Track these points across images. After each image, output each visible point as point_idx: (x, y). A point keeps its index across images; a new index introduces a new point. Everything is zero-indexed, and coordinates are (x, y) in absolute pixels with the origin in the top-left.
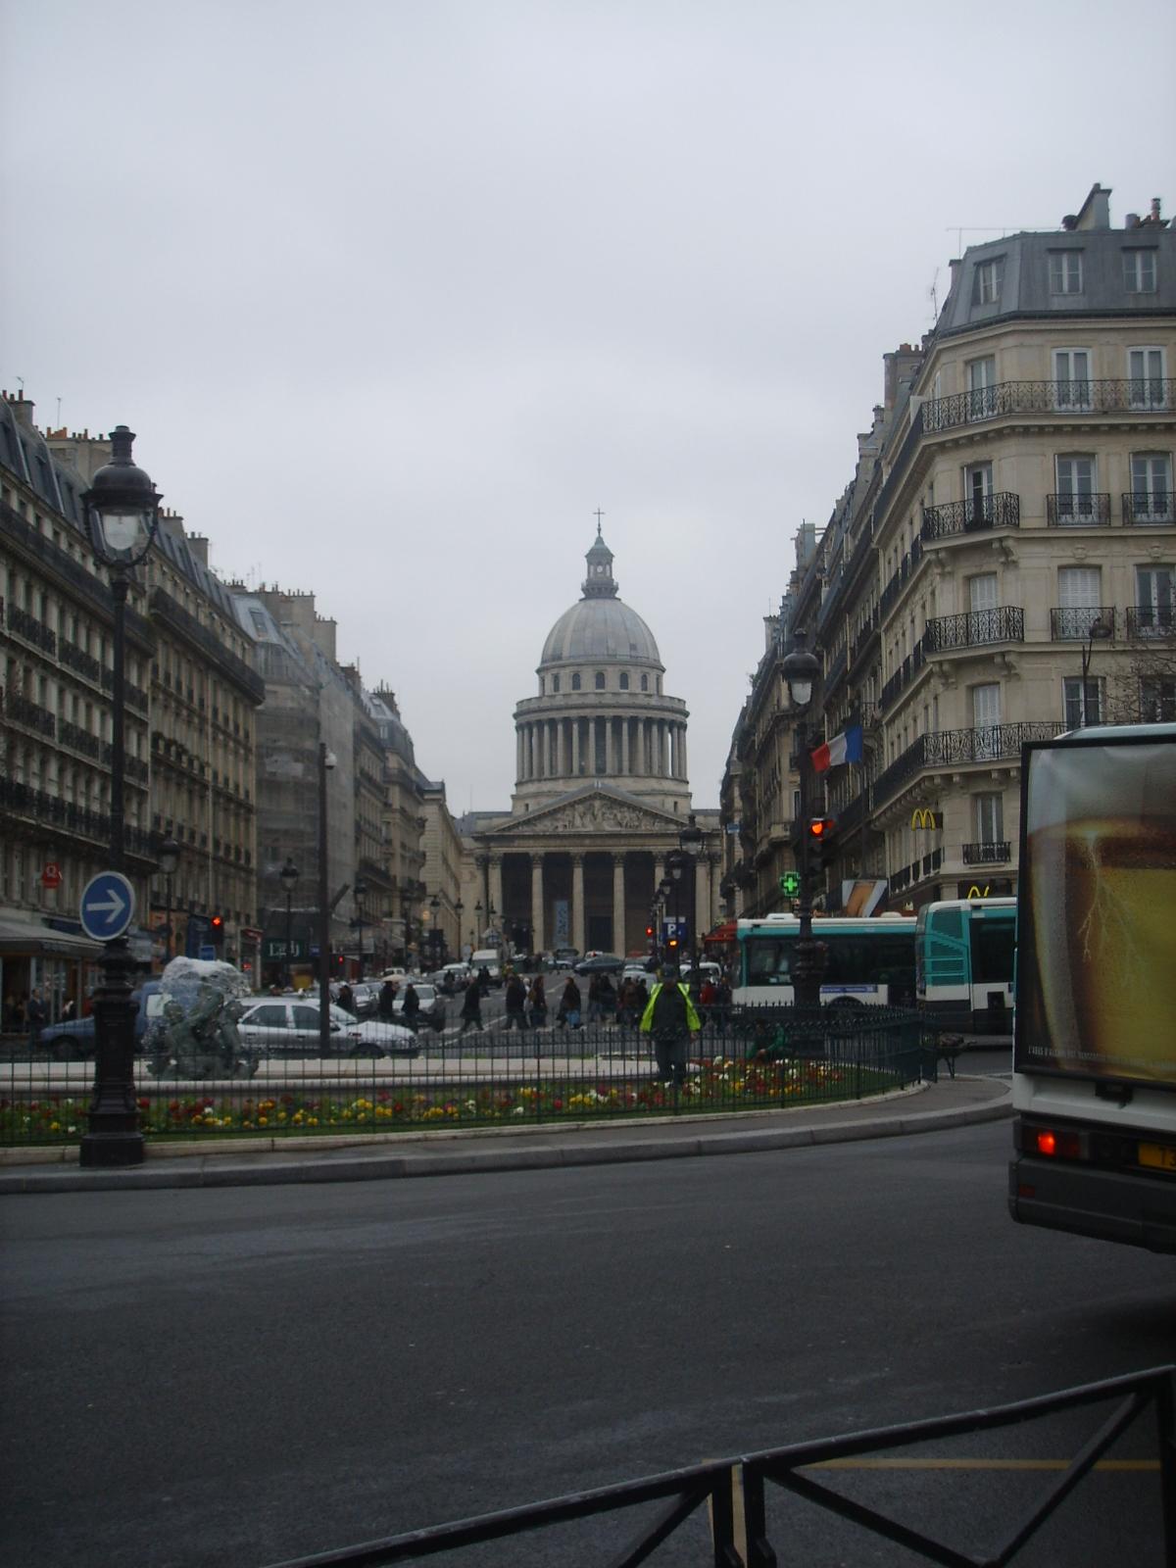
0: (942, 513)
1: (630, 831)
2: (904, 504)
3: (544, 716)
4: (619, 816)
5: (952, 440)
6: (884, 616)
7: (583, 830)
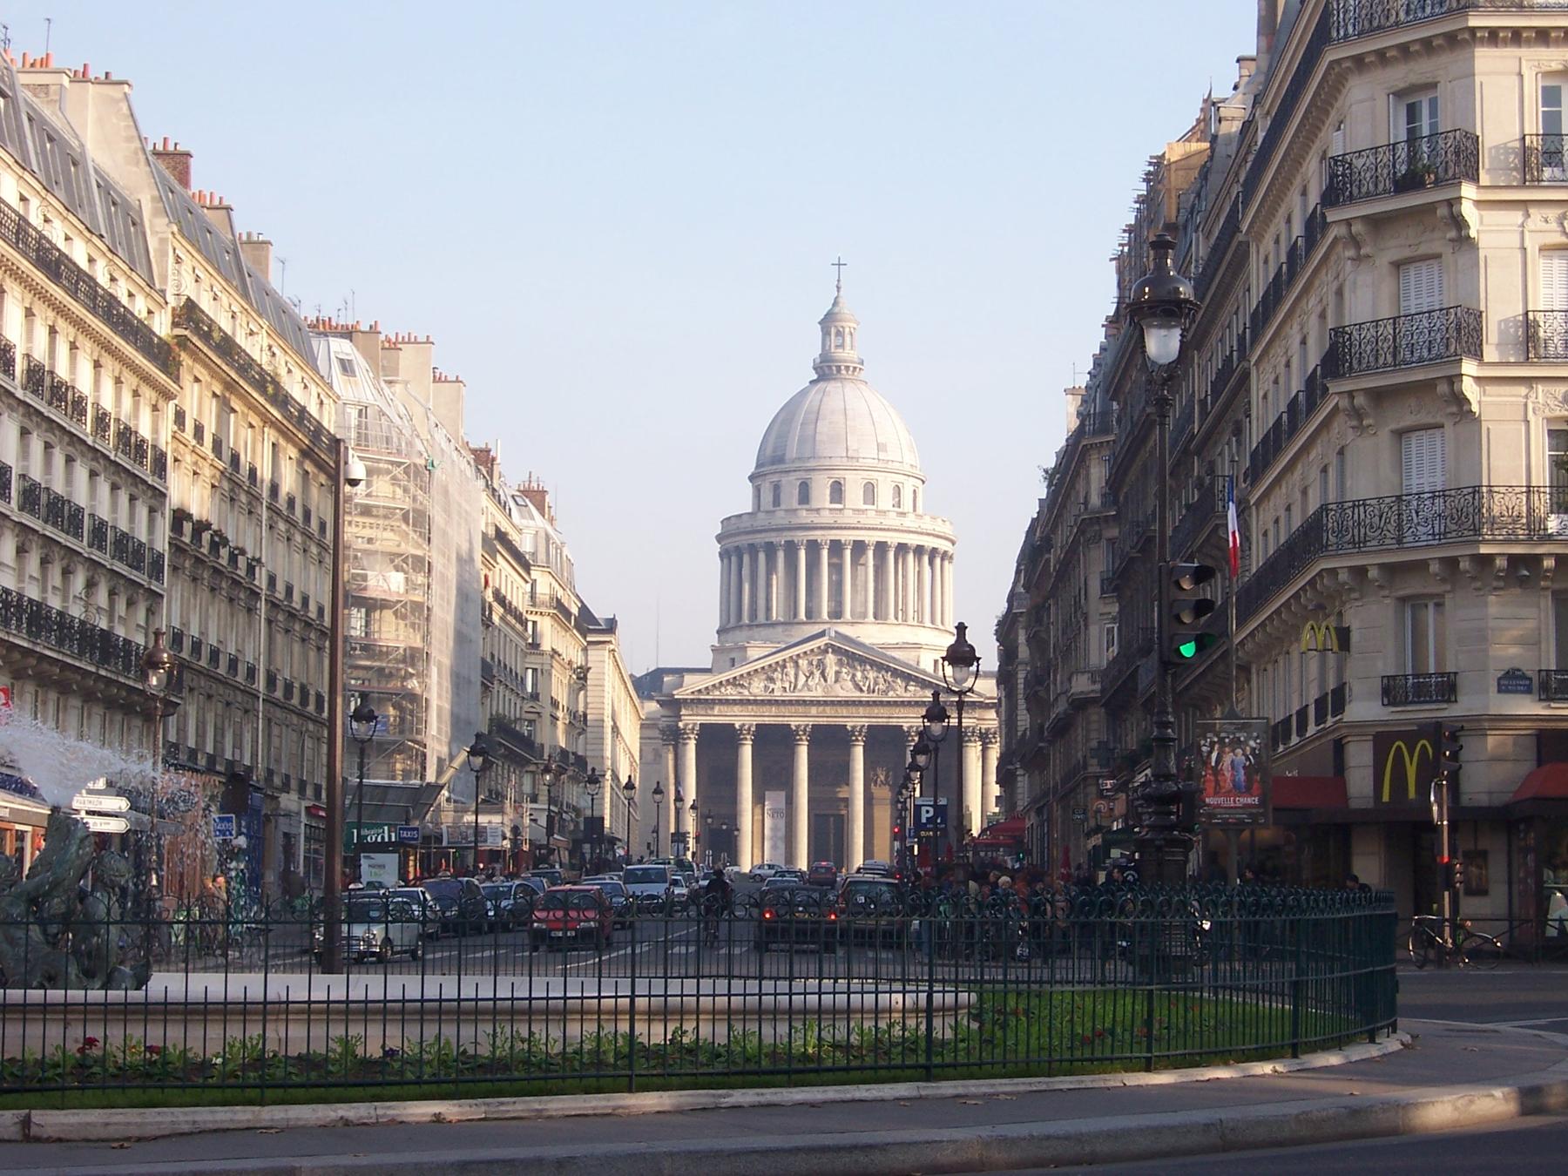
0: (1358, 163)
1: (875, 697)
2: (1295, 160)
3: (759, 539)
4: (859, 675)
5: (1375, 52)
6: (1255, 339)
7: (806, 695)
